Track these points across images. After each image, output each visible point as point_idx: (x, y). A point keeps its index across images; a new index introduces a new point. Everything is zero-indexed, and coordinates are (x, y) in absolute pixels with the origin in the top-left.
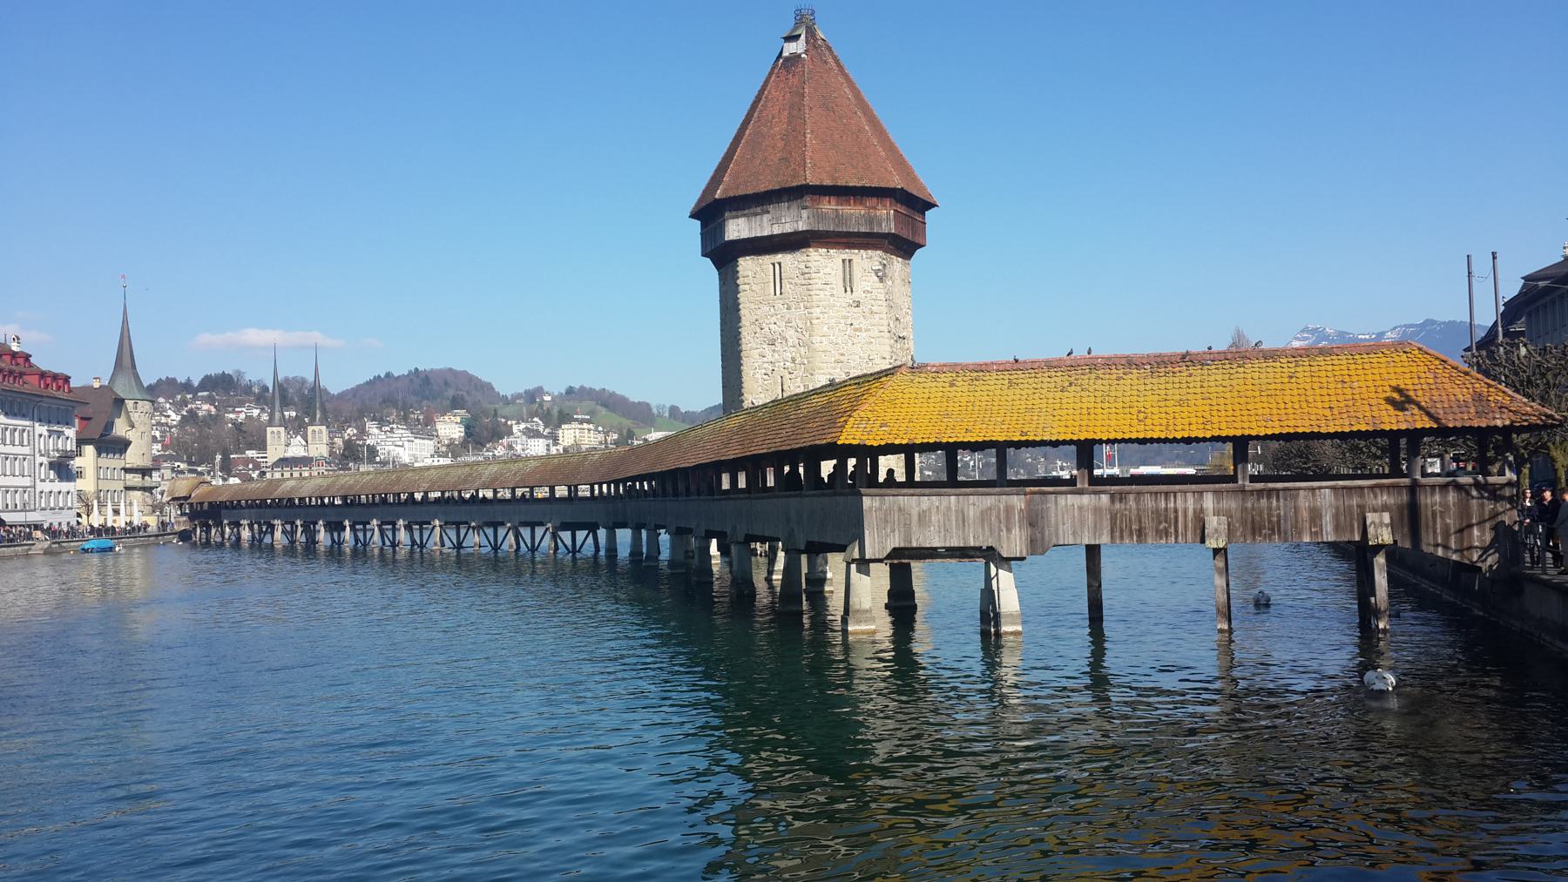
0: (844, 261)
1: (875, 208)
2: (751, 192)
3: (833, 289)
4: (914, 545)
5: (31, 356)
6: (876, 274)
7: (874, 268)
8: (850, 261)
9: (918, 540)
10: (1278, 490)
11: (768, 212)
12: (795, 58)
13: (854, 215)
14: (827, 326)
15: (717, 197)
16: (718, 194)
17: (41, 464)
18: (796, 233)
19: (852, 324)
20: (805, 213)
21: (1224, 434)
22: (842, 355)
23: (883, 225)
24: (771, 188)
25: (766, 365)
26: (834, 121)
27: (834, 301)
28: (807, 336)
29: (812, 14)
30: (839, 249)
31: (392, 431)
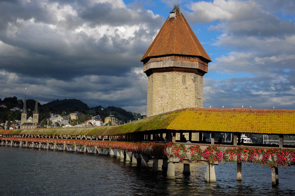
1: (193, 61)
2: (158, 55)
7: (192, 78)
11: (162, 61)
12: (173, 18)
14: (177, 94)
15: (148, 56)
16: (149, 55)
20: (173, 62)
21: (275, 133)
22: (181, 102)
23: (195, 66)
25: (159, 104)
27: (180, 87)
28: (172, 96)
29: (178, 6)
31: (57, 116)
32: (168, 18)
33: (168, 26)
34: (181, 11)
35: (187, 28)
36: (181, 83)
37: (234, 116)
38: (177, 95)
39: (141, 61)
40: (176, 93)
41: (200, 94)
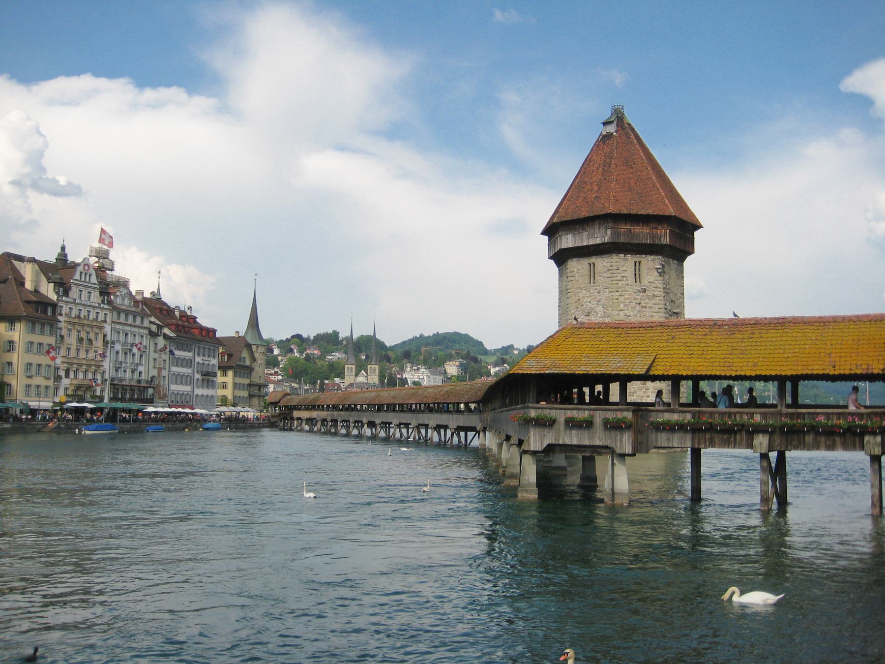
0: (635, 262)
1: (656, 228)
3: (628, 280)
4: (561, 442)
5: (197, 318)
6: (657, 271)
7: (656, 267)
8: (640, 262)
9: (563, 439)
10: (803, 414)
11: (587, 231)
12: (609, 136)
13: (642, 234)
15: (554, 221)
17: (198, 379)
18: (603, 244)
19: (640, 304)
23: (662, 239)
24: (587, 215)
26: (632, 173)
29: (622, 109)
30: (633, 254)
31: (418, 369)
32: (599, 137)
33: (600, 152)
34: (630, 118)
35: (642, 154)
36: (631, 280)
37: (673, 338)
38: (622, 306)
39: (541, 234)
40: (620, 302)
41: (676, 302)
